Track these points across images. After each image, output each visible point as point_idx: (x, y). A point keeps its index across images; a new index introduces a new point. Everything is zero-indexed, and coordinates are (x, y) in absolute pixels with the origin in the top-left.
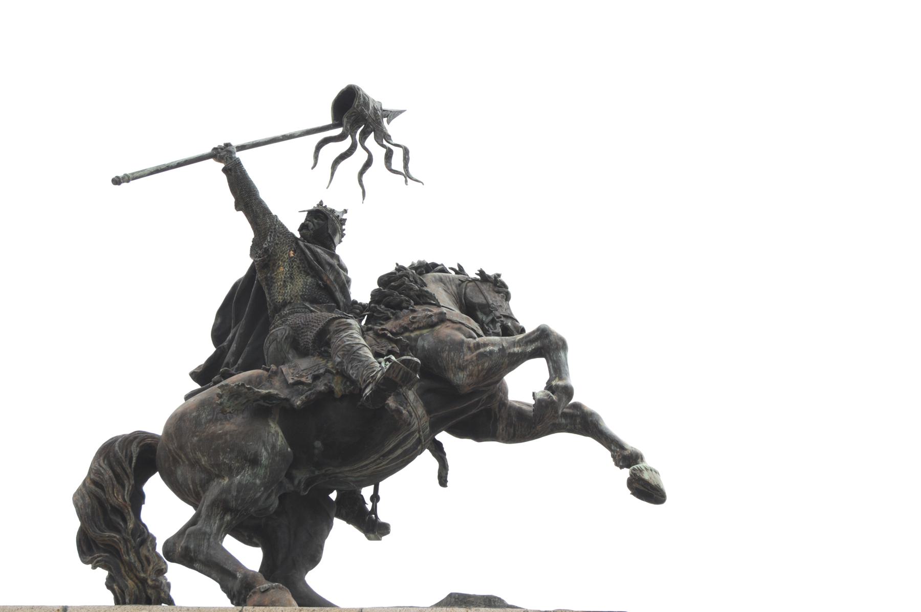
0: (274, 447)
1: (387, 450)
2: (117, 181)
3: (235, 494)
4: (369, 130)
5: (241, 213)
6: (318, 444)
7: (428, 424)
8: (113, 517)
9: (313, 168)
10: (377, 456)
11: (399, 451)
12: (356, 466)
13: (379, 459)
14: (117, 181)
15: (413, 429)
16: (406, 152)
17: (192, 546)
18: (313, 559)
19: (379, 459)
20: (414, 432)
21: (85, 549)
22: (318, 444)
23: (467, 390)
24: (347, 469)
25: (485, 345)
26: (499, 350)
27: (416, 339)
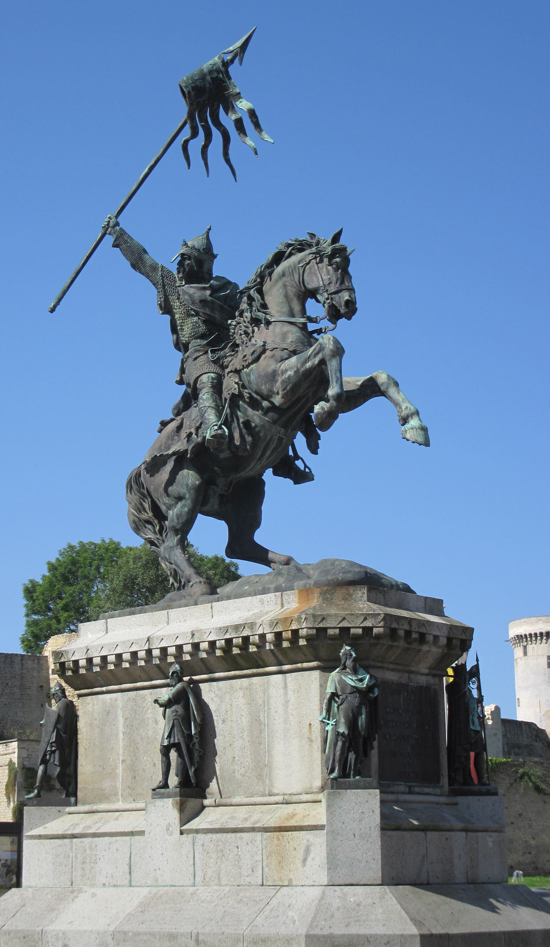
0: (187, 485)
1: (258, 457)
2: (52, 310)
3: (176, 521)
4: (216, 107)
6: (216, 468)
7: (279, 428)
8: (147, 525)
9: (189, 168)
10: (254, 462)
11: (268, 452)
12: (247, 470)
13: (257, 462)
14: (52, 310)
15: (268, 438)
16: (252, 113)
17: (167, 556)
18: (255, 522)
19: (257, 462)
20: (271, 439)
22: (216, 468)
23: (285, 406)
24: (243, 473)
25: (286, 371)
26: (295, 372)
27: (248, 375)
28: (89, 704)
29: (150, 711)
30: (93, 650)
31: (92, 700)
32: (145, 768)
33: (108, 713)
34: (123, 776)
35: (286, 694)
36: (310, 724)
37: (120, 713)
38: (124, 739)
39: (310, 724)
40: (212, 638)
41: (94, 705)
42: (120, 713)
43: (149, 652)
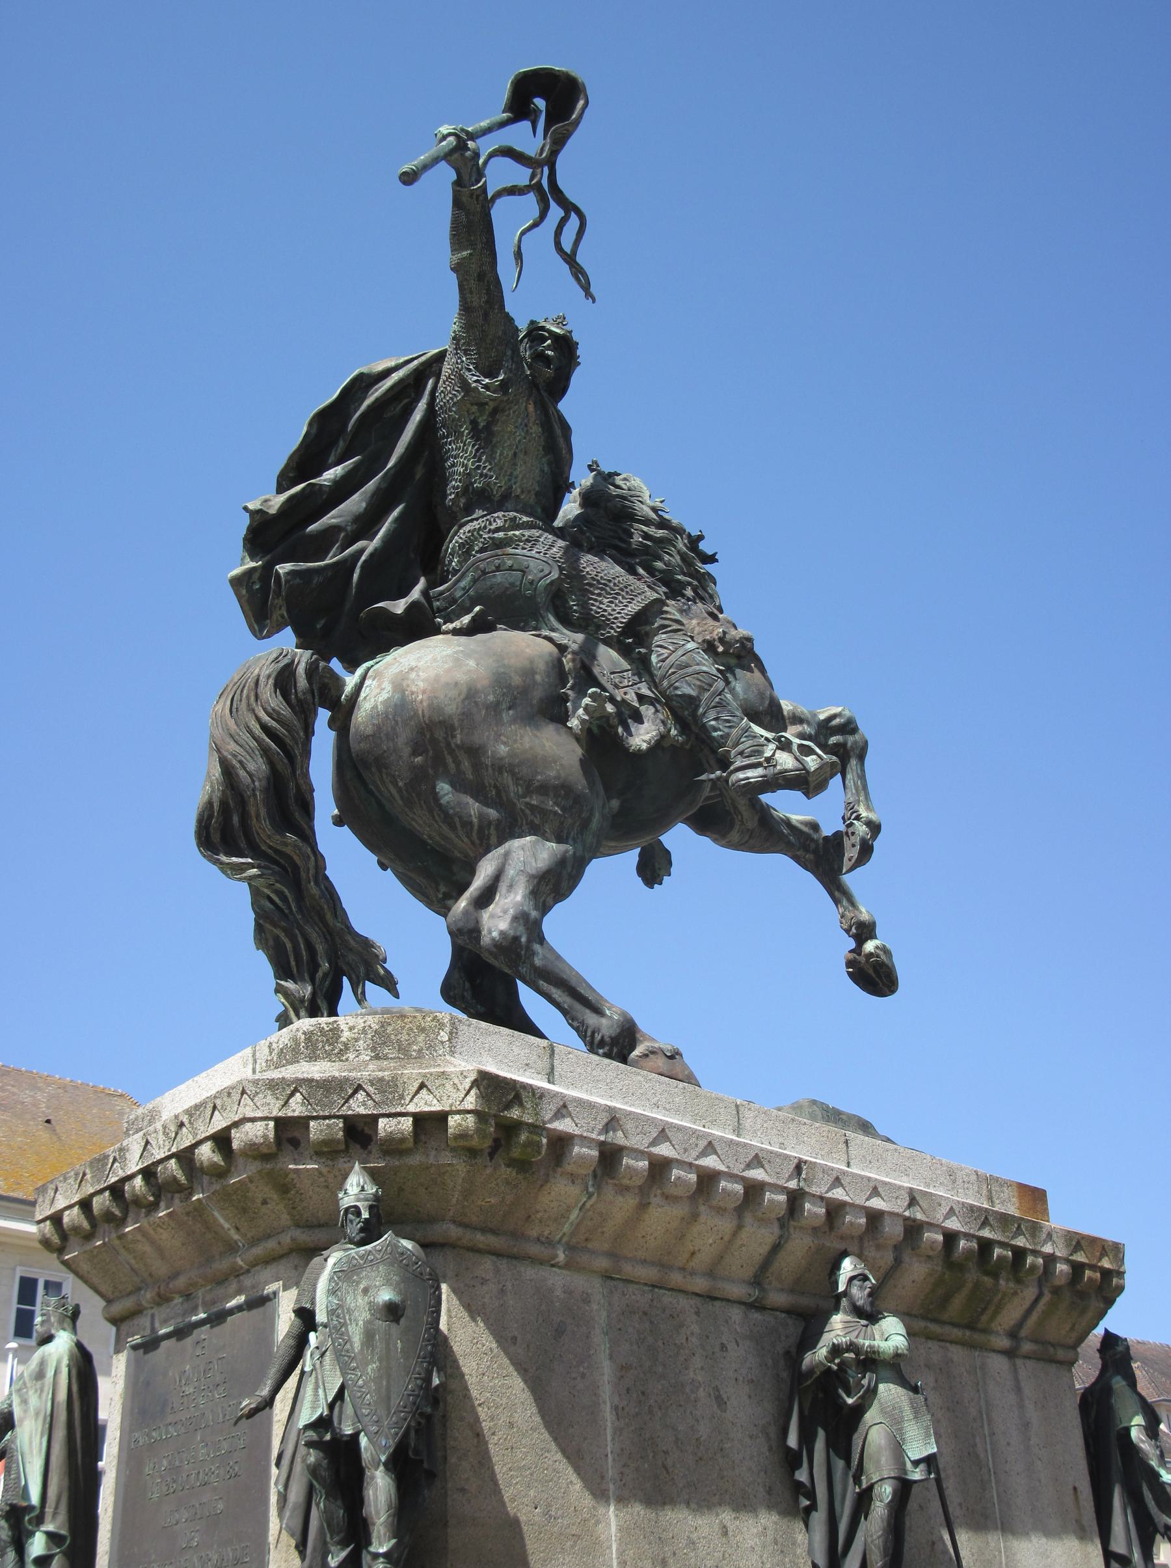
5: (453, 277)
21: (216, 837)
28: (484, 1282)
29: (697, 1361)
30: (629, 1126)
31: (497, 1271)
32: (694, 1536)
33: (559, 1332)
34: (621, 1553)
35: (1021, 1405)
36: (1075, 1489)
37: (601, 1344)
38: (618, 1431)
39: (1075, 1489)
40: (953, 1224)
41: (502, 1291)
42: (601, 1344)
43: (795, 1198)
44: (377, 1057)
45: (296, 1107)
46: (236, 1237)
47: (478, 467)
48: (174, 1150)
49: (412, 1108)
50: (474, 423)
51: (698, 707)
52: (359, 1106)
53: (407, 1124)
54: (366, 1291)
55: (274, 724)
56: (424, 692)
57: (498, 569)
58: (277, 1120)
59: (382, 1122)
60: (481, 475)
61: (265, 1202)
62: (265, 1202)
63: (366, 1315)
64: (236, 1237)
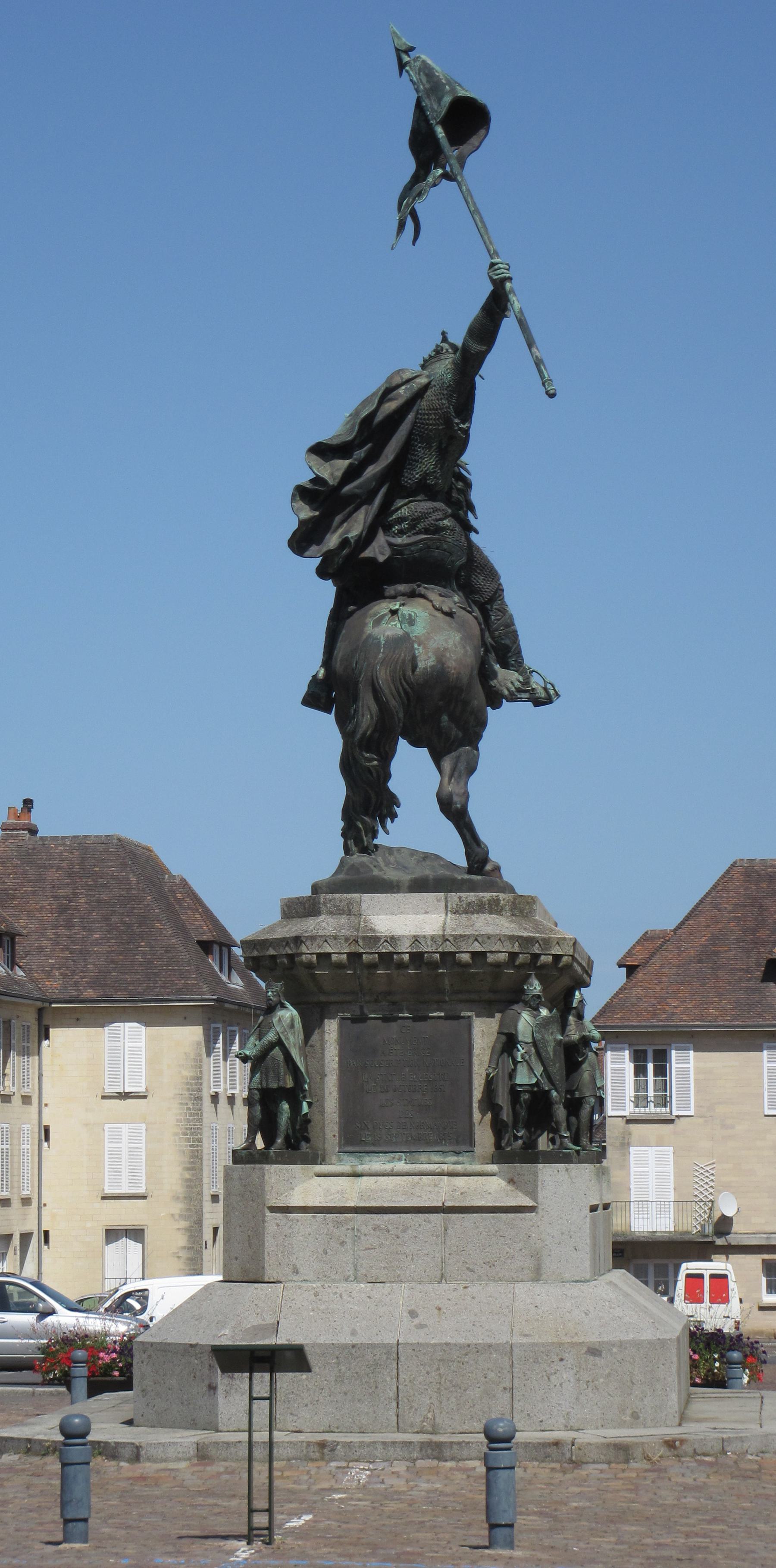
44: (513, 915)
45: (516, 949)
46: (447, 987)
47: (434, 472)
48: (440, 950)
49: (553, 952)
50: (440, 443)
51: (509, 651)
52: (536, 949)
53: (550, 958)
54: (552, 1033)
55: (409, 690)
56: (455, 669)
57: (437, 548)
58: (510, 953)
59: (543, 957)
60: (435, 477)
61: (482, 980)
62: (482, 980)
63: (553, 1044)
64: (447, 987)
